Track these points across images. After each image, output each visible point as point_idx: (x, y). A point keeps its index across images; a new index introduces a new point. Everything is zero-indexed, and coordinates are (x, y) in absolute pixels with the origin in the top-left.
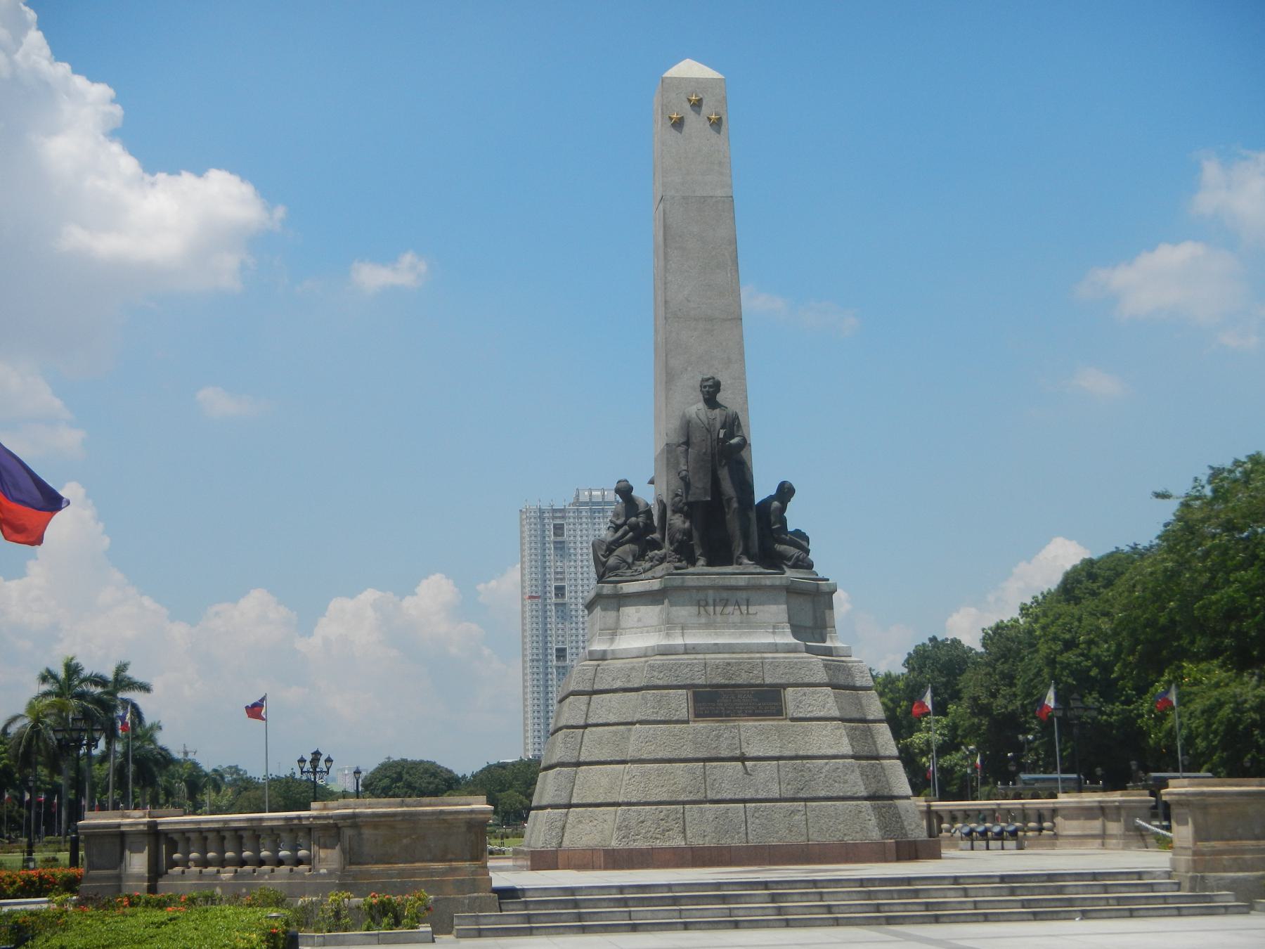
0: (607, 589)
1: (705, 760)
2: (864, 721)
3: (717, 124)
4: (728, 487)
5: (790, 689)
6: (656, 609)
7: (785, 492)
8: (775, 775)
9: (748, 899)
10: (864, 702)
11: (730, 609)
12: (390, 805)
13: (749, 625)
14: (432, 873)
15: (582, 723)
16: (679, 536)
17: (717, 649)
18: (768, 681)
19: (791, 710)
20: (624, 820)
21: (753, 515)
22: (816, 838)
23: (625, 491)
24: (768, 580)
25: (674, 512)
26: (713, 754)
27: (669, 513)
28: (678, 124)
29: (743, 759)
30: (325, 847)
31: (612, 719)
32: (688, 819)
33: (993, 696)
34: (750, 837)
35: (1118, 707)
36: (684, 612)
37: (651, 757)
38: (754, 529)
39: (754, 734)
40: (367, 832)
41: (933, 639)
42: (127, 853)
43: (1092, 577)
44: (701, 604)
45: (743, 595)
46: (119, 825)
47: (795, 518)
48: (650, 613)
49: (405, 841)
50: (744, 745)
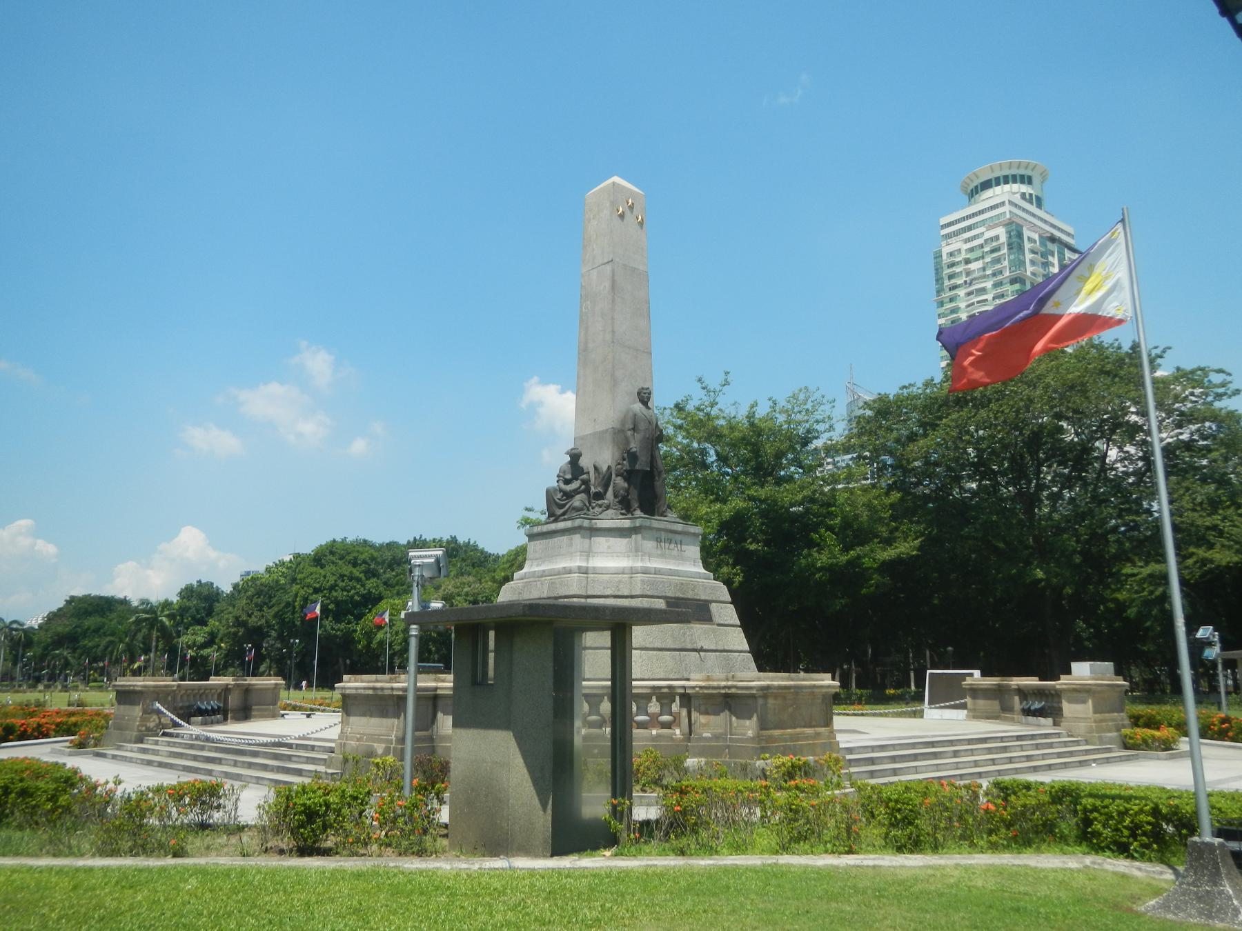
3: (641, 224)
5: (714, 604)
6: (625, 541)
11: (672, 546)
12: (783, 679)
13: (681, 558)
14: (807, 738)
17: (672, 573)
18: (703, 598)
19: (716, 619)
25: (617, 475)
28: (622, 216)
29: (702, 650)
30: (706, 713)
33: (250, 616)
35: (342, 626)
36: (649, 545)
37: (651, 646)
40: (771, 701)
41: (199, 581)
42: (440, 715)
43: (332, 553)
44: (658, 540)
45: (678, 537)
46: (436, 689)
48: (621, 543)
49: (790, 710)
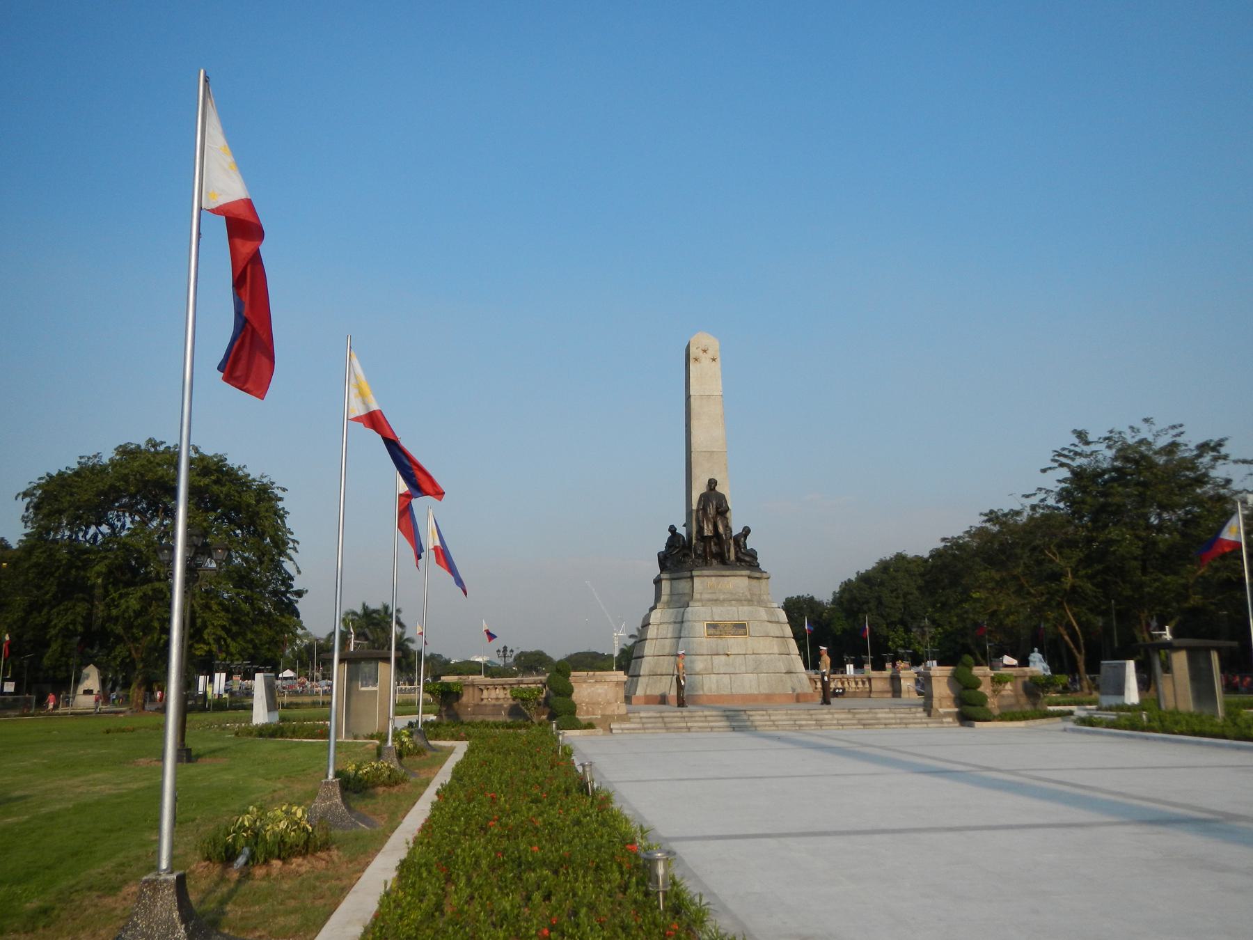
0: (664, 576)
4: (721, 529)
7: (747, 531)
21: (732, 542)
22: (763, 691)
23: (672, 529)
38: (732, 549)
39: (735, 643)
47: (751, 543)
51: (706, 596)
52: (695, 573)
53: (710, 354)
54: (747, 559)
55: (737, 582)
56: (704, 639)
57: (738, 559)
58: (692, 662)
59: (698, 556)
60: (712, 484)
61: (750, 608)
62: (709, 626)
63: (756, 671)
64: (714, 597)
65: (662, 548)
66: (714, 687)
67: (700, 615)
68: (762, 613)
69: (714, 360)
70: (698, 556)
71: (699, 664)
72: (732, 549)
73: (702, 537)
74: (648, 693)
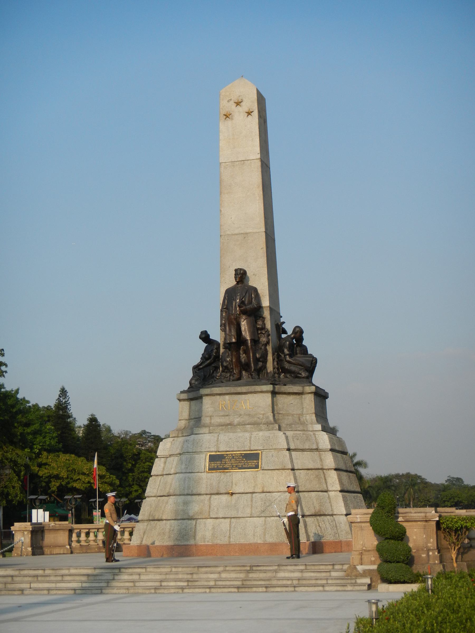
1: (211, 494)
2: (322, 469)
4: (246, 334)
8: (250, 503)
9: (100, 578)
10: (322, 457)
15: (160, 473)
16: (225, 364)
20: (163, 529)
22: (270, 540)
23: (205, 337)
24: (258, 388)
26: (215, 492)
27: (222, 350)
31: (172, 471)
32: (198, 528)
34: (231, 539)
39: (240, 479)
50: (234, 486)
51: (217, 420)
52: (203, 391)
53: (245, 106)
54: (293, 368)
55: (257, 401)
56: (204, 475)
57: (281, 368)
58: (186, 503)
59: (226, 369)
60: (241, 275)
61: (267, 433)
62: (213, 458)
63: (264, 514)
64: (226, 420)
65: (197, 360)
66: (208, 534)
67: (212, 441)
68: (280, 439)
69: (249, 113)
70: (226, 369)
71: (196, 506)
72: (270, 357)
73: (228, 346)
74: (144, 543)
